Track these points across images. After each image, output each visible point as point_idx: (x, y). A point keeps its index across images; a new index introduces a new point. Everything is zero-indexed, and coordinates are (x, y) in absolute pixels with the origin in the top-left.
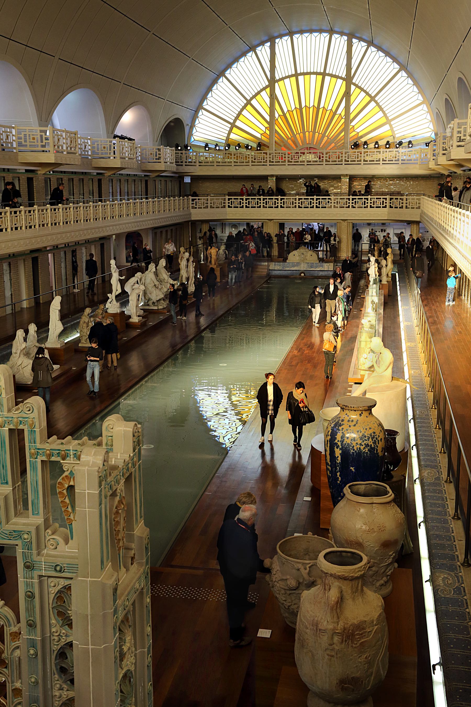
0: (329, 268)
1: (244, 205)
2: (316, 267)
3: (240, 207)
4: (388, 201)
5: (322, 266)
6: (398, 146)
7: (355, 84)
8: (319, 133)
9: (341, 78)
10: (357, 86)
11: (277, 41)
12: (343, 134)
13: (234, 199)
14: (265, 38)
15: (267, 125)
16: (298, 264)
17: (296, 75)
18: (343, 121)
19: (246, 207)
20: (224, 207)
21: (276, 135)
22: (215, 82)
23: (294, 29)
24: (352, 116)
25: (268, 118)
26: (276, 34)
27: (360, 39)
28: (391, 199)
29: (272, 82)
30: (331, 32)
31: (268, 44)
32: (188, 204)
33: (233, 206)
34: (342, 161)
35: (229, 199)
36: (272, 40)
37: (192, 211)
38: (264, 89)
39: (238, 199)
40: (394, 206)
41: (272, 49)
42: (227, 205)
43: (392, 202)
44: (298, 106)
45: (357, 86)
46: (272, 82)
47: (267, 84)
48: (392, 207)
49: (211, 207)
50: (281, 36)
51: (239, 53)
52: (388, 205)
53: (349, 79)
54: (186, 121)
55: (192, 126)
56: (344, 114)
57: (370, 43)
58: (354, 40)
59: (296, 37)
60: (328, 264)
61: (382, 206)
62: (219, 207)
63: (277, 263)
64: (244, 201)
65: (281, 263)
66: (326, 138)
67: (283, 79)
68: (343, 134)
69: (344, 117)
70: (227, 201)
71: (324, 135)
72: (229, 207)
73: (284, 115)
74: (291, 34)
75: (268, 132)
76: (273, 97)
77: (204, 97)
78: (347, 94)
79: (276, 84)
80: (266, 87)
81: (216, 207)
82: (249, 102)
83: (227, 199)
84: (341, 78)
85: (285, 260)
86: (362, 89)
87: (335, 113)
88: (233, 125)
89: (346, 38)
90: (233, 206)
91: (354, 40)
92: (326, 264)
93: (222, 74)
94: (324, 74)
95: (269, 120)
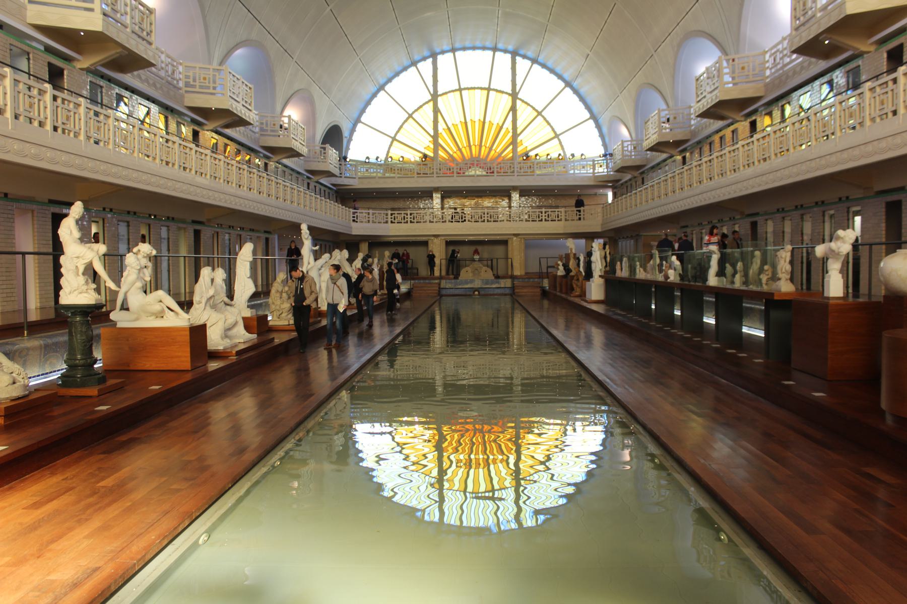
0: (505, 284)
1: (409, 220)
2: (492, 284)
3: (404, 223)
4: (563, 214)
5: (498, 283)
6: (571, 157)
7: (520, 99)
8: (486, 147)
9: (506, 93)
10: (523, 101)
11: (440, 57)
12: (511, 147)
13: (398, 214)
14: (426, 53)
15: (431, 139)
16: (472, 281)
17: (460, 90)
18: (510, 134)
19: (411, 222)
20: (387, 222)
21: (440, 148)
22: (374, 95)
23: (457, 45)
24: (518, 132)
25: (432, 134)
26: (438, 50)
27: (524, 57)
28: (566, 212)
29: (435, 96)
30: (495, 49)
31: (430, 60)
32: (349, 217)
33: (396, 221)
34: (513, 172)
35: (392, 215)
36: (434, 56)
37: (354, 225)
38: (427, 103)
39: (401, 214)
40: (570, 219)
42: (389, 220)
43: (567, 214)
45: (523, 101)
46: (435, 96)
47: (430, 98)
48: (568, 220)
49: (373, 222)
50: (443, 52)
51: (401, 68)
52: (563, 218)
53: (514, 95)
54: (346, 133)
55: (350, 140)
56: (511, 127)
57: (534, 61)
58: (518, 59)
59: (458, 53)
60: (505, 280)
61: (557, 219)
62: (381, 223)
63: (448, 281)
64: (409, 216)
65: (453, 281)
66: (493, 152)
68: (511, 147)
69: (511, 131)
70: (389, 216)
71: (491, 149)
72: (392, 222)
73: (449, 129)
74: (453, 50)
75: (432, 146)
76: (436, 111)
77: (363, 111)
78: (513, 109)
79: (439, 98)
80: (429, 101)
81: (379, 223)
82: (410, 116)
83: (389, 214)
84: (506, 93)
85: (457, 276)
86: (528, 104)
87: (501, 128)
89: (509, 56)
90: (396, 221)
91: (518, 59)
92: (503, 280)
93: (382, 88)
94: (489, 89)
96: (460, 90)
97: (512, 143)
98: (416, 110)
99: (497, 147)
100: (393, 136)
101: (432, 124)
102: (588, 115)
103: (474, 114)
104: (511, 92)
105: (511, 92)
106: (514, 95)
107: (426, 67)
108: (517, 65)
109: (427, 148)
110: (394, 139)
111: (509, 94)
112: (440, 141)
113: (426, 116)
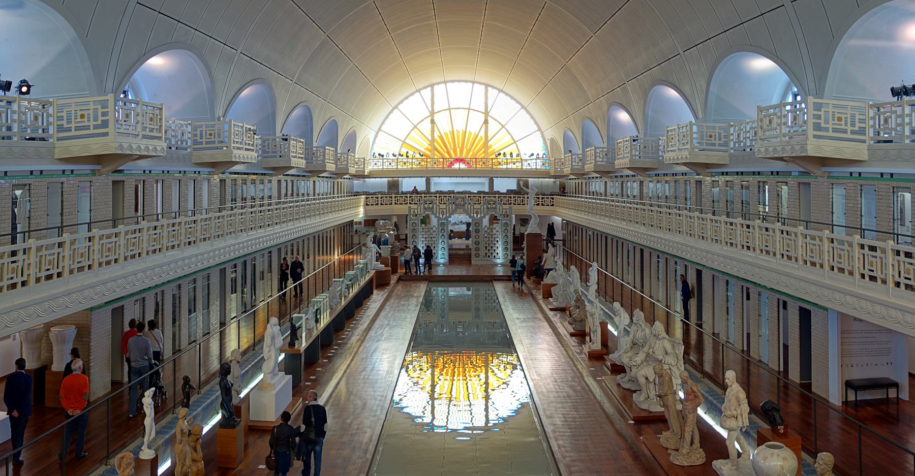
11: (436, 87)
12: (483, 150)
14: (426, 84)
17: (450, 109)
18: (483, 140)
22: (391, 112)
24: (489, 139)
25: (430, 138)
26: (434, 81)
29: (432, 113)
30: (474, 82)
36: (432, 86)
41: (432, 91)
44: (451, 130)
46: (432, 113)
47: (429, 114)
50: (438, 84)
53: (486, 113)
55: (374, 142)
57: (501, 91)
67: (438, 112)
71: (470, 151)
75: (430, 147)
78: (486, 122)
79: (435, 115)
80: (429, 116)
88: (404, 142)
89: (483, 87)
93: (396, 107)
94: (469, 109)
95: (430, 139)
96: (450, 109)
97: (484, 147)
98: (419, 123)
99: (474, 149)
100: (403, 140)
101: (430, 132)
102: (537, 129)
103: (459, 126)
104: (484, 111)
105: (484, 111)
106: (486, 113)
107: (427, 93)
108: (489, 93)
109: (427, 149)
110: (404, 142)
111: (483, 113)
112: (436, 144)
113: (426, 126)
